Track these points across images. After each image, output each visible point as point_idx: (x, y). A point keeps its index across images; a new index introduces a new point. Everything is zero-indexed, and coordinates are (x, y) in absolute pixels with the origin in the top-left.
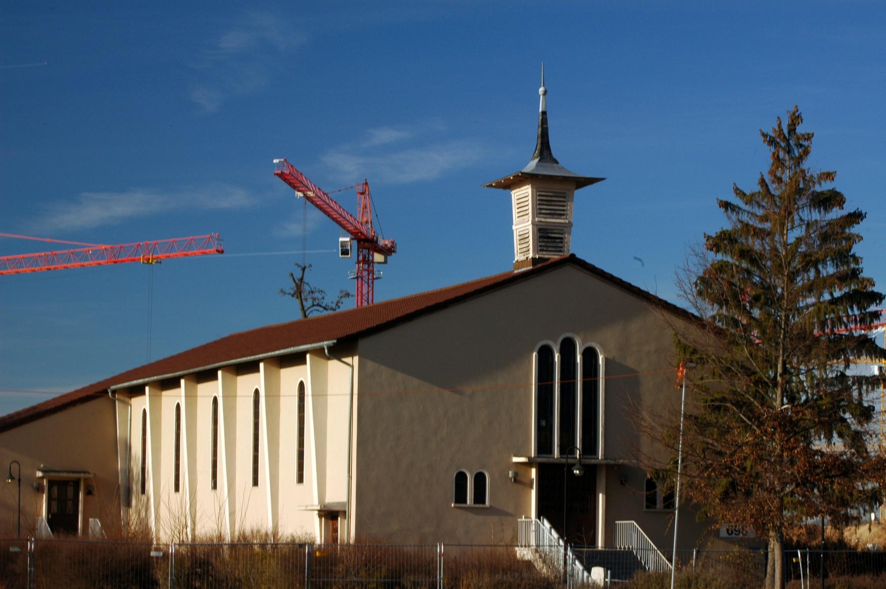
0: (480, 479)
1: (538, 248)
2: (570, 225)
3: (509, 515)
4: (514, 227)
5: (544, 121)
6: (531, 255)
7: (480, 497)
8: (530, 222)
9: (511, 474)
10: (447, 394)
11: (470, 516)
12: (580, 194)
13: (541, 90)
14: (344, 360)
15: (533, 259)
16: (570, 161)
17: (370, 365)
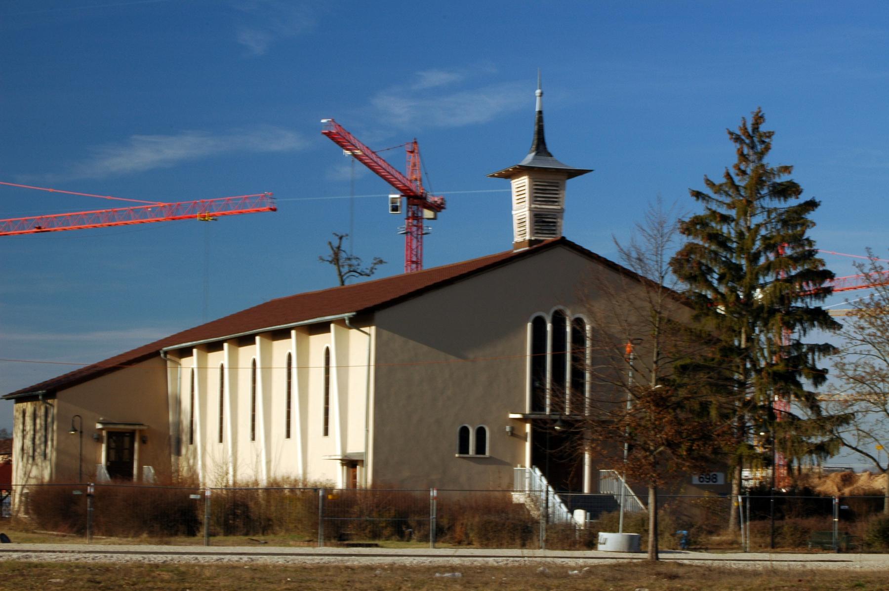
0: (481, 433)
1: (534, 231)
2: (562, 211)
3: (508, 464)
4: (514, 212)
5: (540, 120)
6: (528, 237)
7: (480, 449)
8: (527, 209)
9: (508, 429)
10: (452, 358)
11: (472, 464)
12: (570, 183)
13: (538, 92)
14: (362, 329)
15: (530, 241)
16: (563, 155)
17: (386, 334)
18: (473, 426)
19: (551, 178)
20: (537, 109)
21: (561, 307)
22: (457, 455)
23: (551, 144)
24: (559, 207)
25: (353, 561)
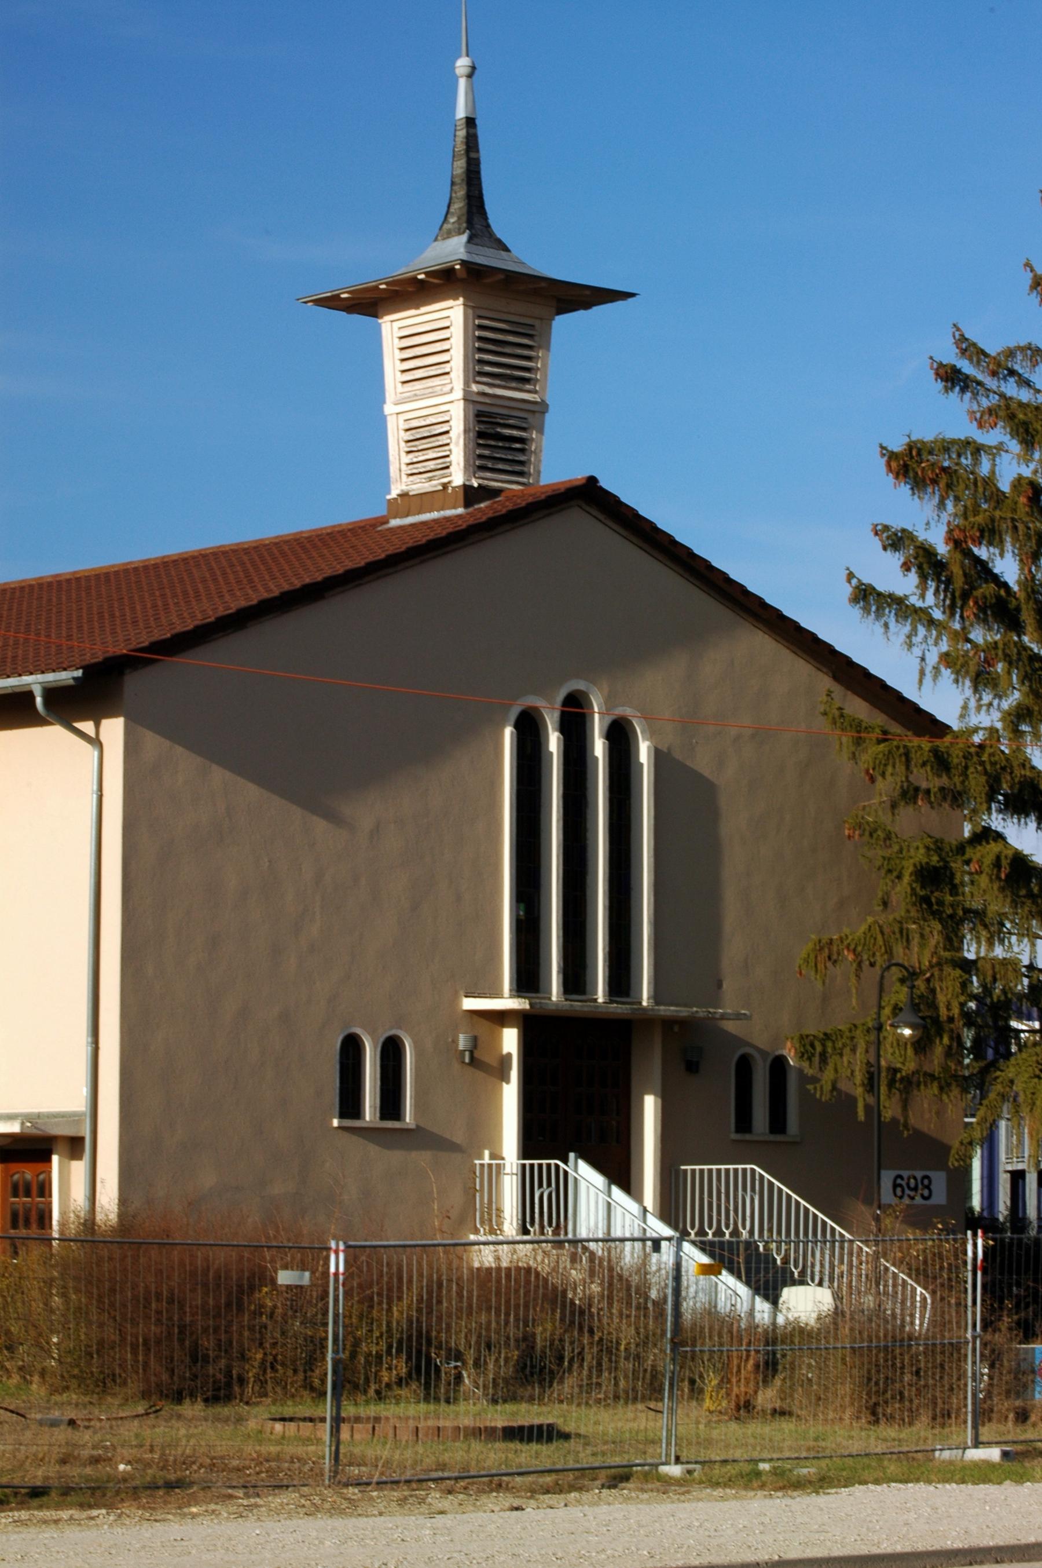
0: (392, 1053)
1: (477, 463)
2: (541, 408)
3: (454, 1145)
4: (389, 409)
5: (472, 143)
6: (457, 477)
7: (391, 1103)
8: (458, 394)
9: (462, 1042)
10: (320, 826)
11: (373, 1150)
12: (566, 326)
13: (462, 64)
14: (77, 725)
15: (467, 488)
16: (536, 248)
17: (152, 742)
18: (372, 1034)
19: (519, 309)
20: (461, 113)
21: (577, 685)
22: (335, 1123)
23: (500, 217)
24: (536, 398)
25: (537, 1454)
